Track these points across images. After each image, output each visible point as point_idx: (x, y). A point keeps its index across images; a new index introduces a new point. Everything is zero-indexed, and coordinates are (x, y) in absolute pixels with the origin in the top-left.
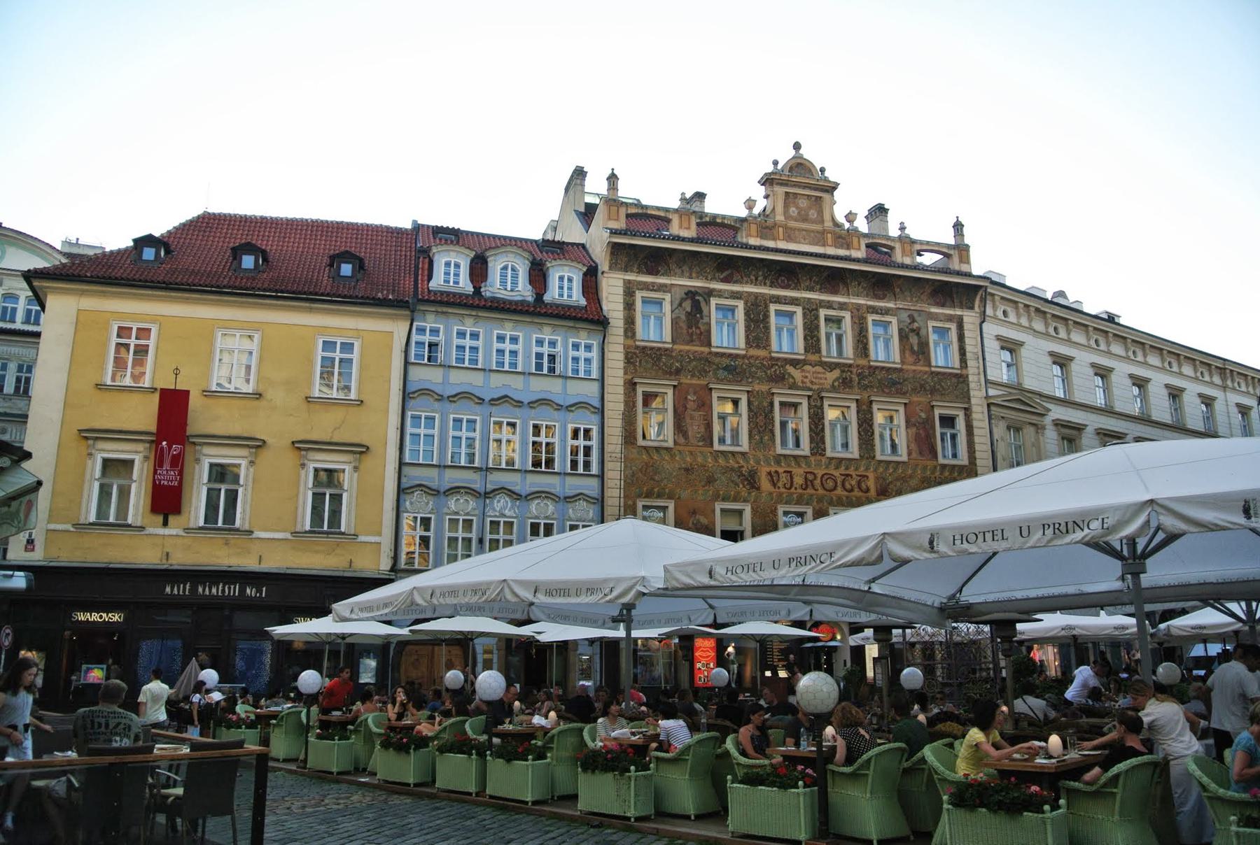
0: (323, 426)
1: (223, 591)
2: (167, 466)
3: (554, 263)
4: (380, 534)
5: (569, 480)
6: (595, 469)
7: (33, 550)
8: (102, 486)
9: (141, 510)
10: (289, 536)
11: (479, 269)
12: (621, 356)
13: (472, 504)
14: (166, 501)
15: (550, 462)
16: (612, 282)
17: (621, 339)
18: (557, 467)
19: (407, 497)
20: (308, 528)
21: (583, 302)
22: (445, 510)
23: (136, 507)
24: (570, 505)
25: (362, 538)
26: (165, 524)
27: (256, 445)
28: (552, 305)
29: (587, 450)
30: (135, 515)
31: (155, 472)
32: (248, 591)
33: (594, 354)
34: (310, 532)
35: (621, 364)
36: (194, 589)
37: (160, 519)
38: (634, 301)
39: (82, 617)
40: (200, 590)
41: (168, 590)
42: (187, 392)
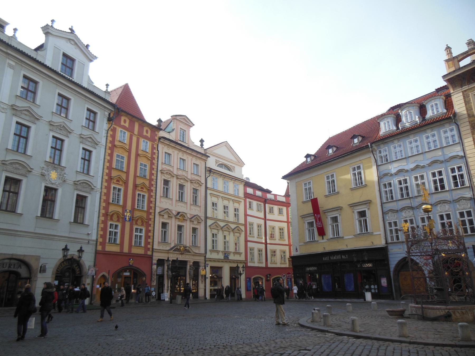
2: (318, 222)
3: (426, 102)
4: (380, 231)
5: (454, 192)
6: (467, 184)
10: (353, 237)
11: (398, 119)
12: (469, 127)
13: (411, 213)
14: (322, 232)
15: (443, 187)
16: (455, 96)
17: (467, 120)
18: (447, 188)
19: (387, 215)
20: (359, 233)
21: (445, 111)
22: (402, 217)
24: (457, 203)
25: (375, 233)
26: (323, 239)
27: (339, 209)
28: (431, 118)
29: (462, 176)
33: (455, 132)
34: (359, 234)
35: (470, 131)
36: (330, 258)
37: (321, 237)
38: (470, 99)
39: (308, 269)
42: (316, 199)
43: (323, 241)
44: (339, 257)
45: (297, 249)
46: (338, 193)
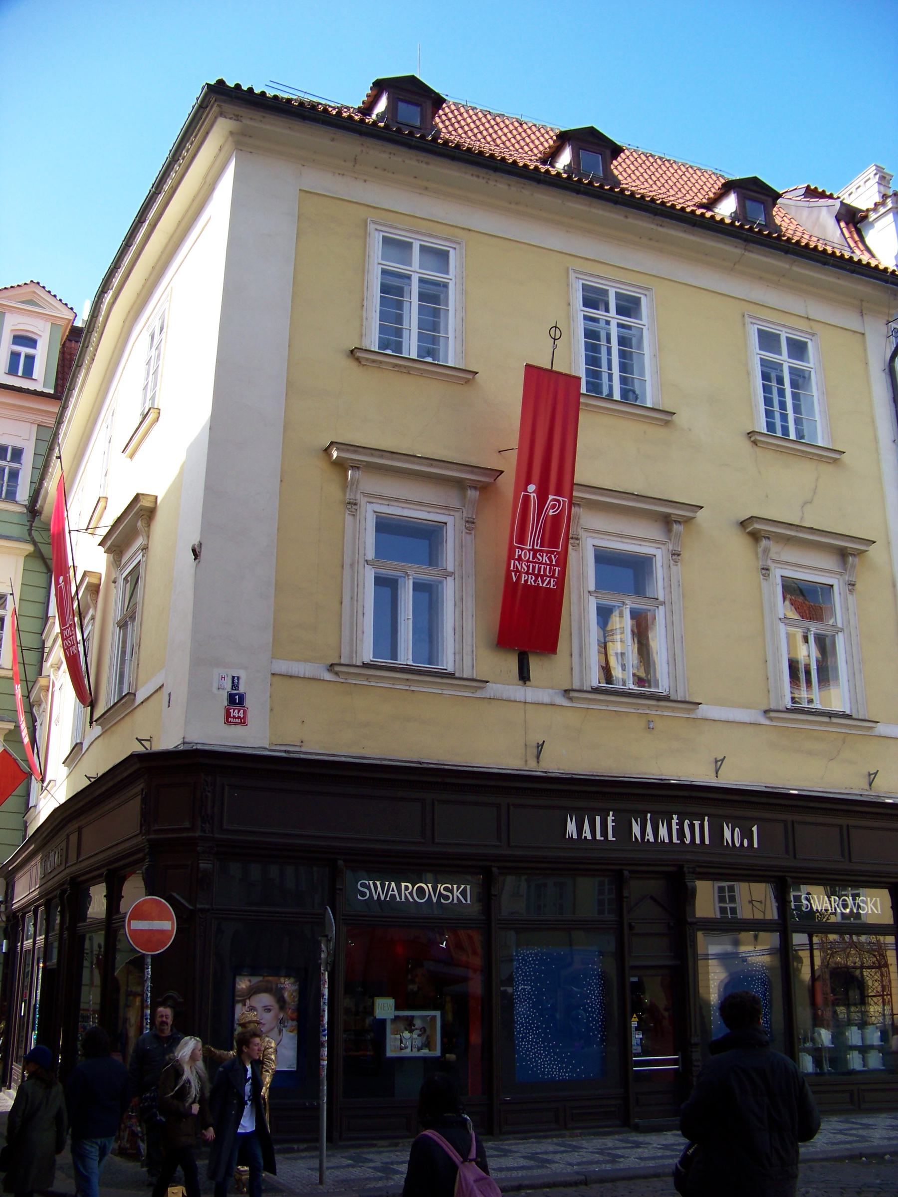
0: (786, 491)
1: (681, 832)
7: (243, 722)
8: (380, 581)
9: (468, 639)
14: (528, 624)
23: (459, 631)
25: (882, 729)
26: (524, 676)
27: (672, 518)
30: (459, 653)
31: (511, 556)
32: (727, 834)
36: (623, 829)
37: (511, 663)
40: (636, 829)
41: (571, 827)
43: (519, 692)
44: (698, 832)
45: (236, 700)
46: (664, 417)
